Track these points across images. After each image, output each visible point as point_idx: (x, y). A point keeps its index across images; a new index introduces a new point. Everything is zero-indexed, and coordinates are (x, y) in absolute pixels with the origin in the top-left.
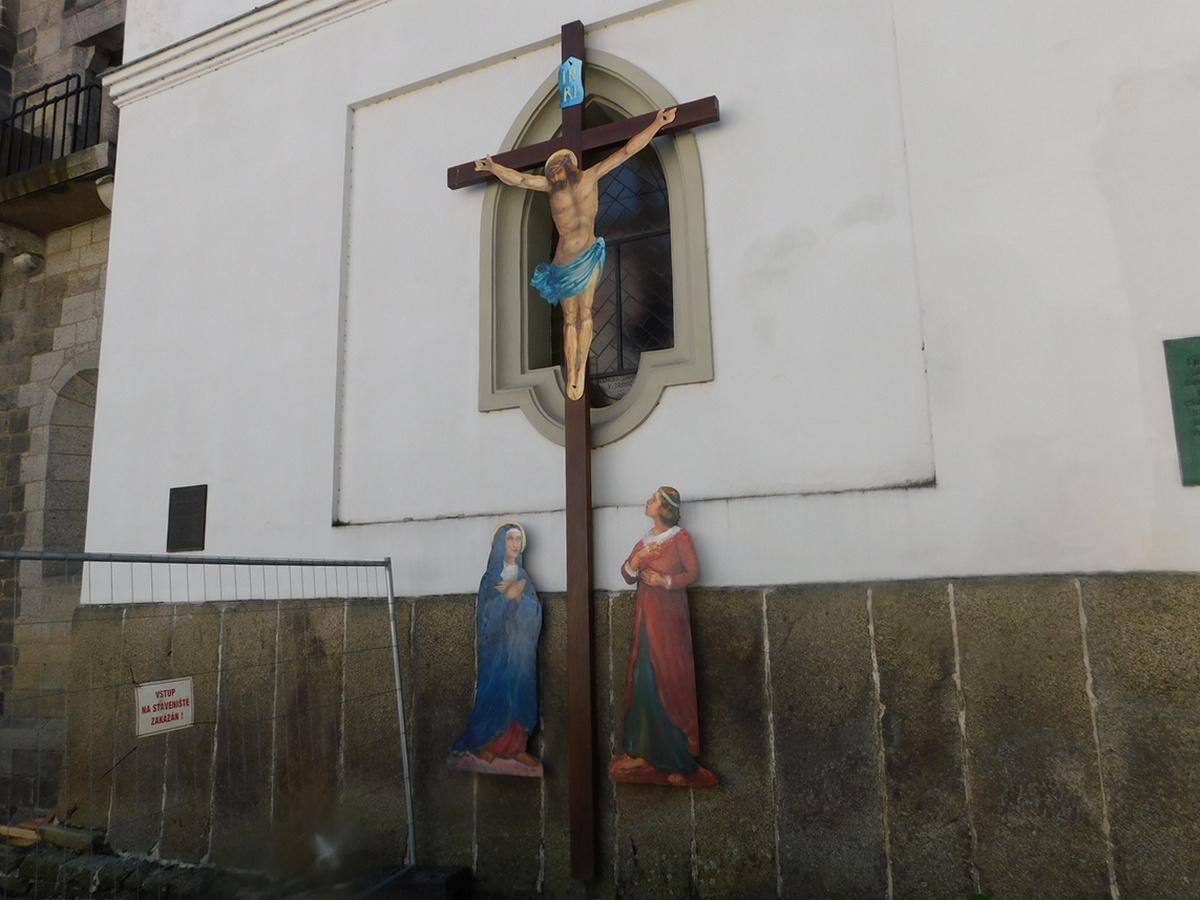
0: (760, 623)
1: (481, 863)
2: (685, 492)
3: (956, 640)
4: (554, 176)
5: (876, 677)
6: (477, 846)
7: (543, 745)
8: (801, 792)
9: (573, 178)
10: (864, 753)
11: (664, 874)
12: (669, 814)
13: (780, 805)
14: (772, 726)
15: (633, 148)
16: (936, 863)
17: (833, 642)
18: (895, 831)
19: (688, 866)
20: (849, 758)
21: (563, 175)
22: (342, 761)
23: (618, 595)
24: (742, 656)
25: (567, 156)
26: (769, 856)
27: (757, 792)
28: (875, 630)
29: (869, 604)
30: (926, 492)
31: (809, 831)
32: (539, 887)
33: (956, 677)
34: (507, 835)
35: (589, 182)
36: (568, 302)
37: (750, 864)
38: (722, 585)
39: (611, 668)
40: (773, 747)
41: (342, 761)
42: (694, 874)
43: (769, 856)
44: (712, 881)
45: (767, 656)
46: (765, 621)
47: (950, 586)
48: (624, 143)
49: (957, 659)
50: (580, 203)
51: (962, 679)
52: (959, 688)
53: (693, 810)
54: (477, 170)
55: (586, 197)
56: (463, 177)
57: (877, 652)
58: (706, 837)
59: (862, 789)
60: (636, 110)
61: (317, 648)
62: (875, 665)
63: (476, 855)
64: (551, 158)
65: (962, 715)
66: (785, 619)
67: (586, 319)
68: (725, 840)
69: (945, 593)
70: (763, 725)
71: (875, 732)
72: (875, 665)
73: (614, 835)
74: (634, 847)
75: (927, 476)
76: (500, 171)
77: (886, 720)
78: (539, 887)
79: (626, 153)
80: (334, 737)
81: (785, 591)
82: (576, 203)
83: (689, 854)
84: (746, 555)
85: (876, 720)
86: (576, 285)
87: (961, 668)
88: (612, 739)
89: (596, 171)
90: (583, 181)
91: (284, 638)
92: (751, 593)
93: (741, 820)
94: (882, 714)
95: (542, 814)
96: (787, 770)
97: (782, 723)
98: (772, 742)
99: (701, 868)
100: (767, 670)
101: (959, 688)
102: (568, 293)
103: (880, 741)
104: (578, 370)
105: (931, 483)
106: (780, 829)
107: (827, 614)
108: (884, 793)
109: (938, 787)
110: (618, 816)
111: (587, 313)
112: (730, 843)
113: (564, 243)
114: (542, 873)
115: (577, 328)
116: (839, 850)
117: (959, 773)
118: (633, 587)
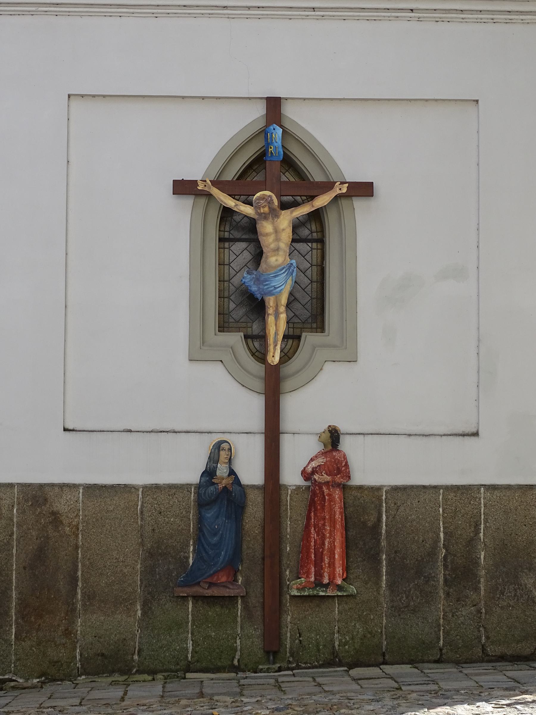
0: (381, 506)
1: (194, 652)
2: (342, 427)
3: (483, 517)
4: (260, 209)
5: (442, 535)
6: (191, 642)
7: (241, 578)
8: (398, 595)
9: (273, 214)
10: (433, 575)
11: (318, 646)
12: (322, 613)
13: (387, 604)
14: (384, 562)
15: (317, 204)
16: (465, 626)
17: (421, 517)
18: (446, 613)
19: (332, 641)
20: (425, 577)
21: (266, 209)
22: (79, 596)
23: (294, 488)
24: (370, 524)
25: (270, 196)
26: (379, 631)
27: (375, 598)
28: (443, 511)
29: (441, 497)
30: (473, 439)
31: (402, 616)
32: (236, 662)
33: (481, 535)
34: (214, 634)
35: (286, 220)
36: (269, 299)
37: (369, 636)
38: (358, 484)
39: (289, 530)
40: (384, 574)
41: (79, 596)
42: (337, 643)
43: (379, 631)
44: (347, 647)
45: (384, 524)
46: (384, 505)
47: (482, 489)
48: (312, 198)
49: (482, 526)
50: (277, 231)
51: (484, 536)
52: (482, 541)
53: (337, 609)
54: (199, 188)
55: (283, 230)
56: (183, 188)
57: (443, 522)
58: (344, 624)
59: (430, 592)
60: (318, 177)
61: (56, 518)
62: (442, 529)
63: (191, 648)
64: (258, 194)
65: (483, 553)
66: (395, 504)
67: (282, 313)
68: (355, 624)
69: (479, 492)
70: (380, 562)
71: (439, 564)
72: (442, 529)
73: (287, 627)
74: (299, 633)
75: (474, 430)
76: (215, 192)
77: (445, 558)
78: (236, 662)
79: (313, 206)
80: (74, 580)
81: (396, 489)
82: (276, 231)
83: (334, 634)
84: (371, 467)
85: (440, 558)
86: (275, 288)
87: (484, 530)
88: (287, 573)
89: (291, 213)
90: (282, 217)
91: (22, 512)
92: (376, 490)
93: (365, 613)
94: (444, 554)
95: (239, 619)
96: (391, 586)
97: (390, 562)
98: (384, 571)
99: (340, 641)
100: (383, 532)
101: (482, 541)
102: (270, 293)
103: (441, 568)
104: (276, 346)
105: (476, 434)
106: (386, 616)
107: (419, 502)
108: (442, 594)
109: (468, 590)
110: (289, 617)
111: (282, 309)
112: (358, 626)
113: (267, 258)
114: (238, 653)
115: (275, 318)
116: (417, 624)
117: (479, 582)
118: (308, 483)
